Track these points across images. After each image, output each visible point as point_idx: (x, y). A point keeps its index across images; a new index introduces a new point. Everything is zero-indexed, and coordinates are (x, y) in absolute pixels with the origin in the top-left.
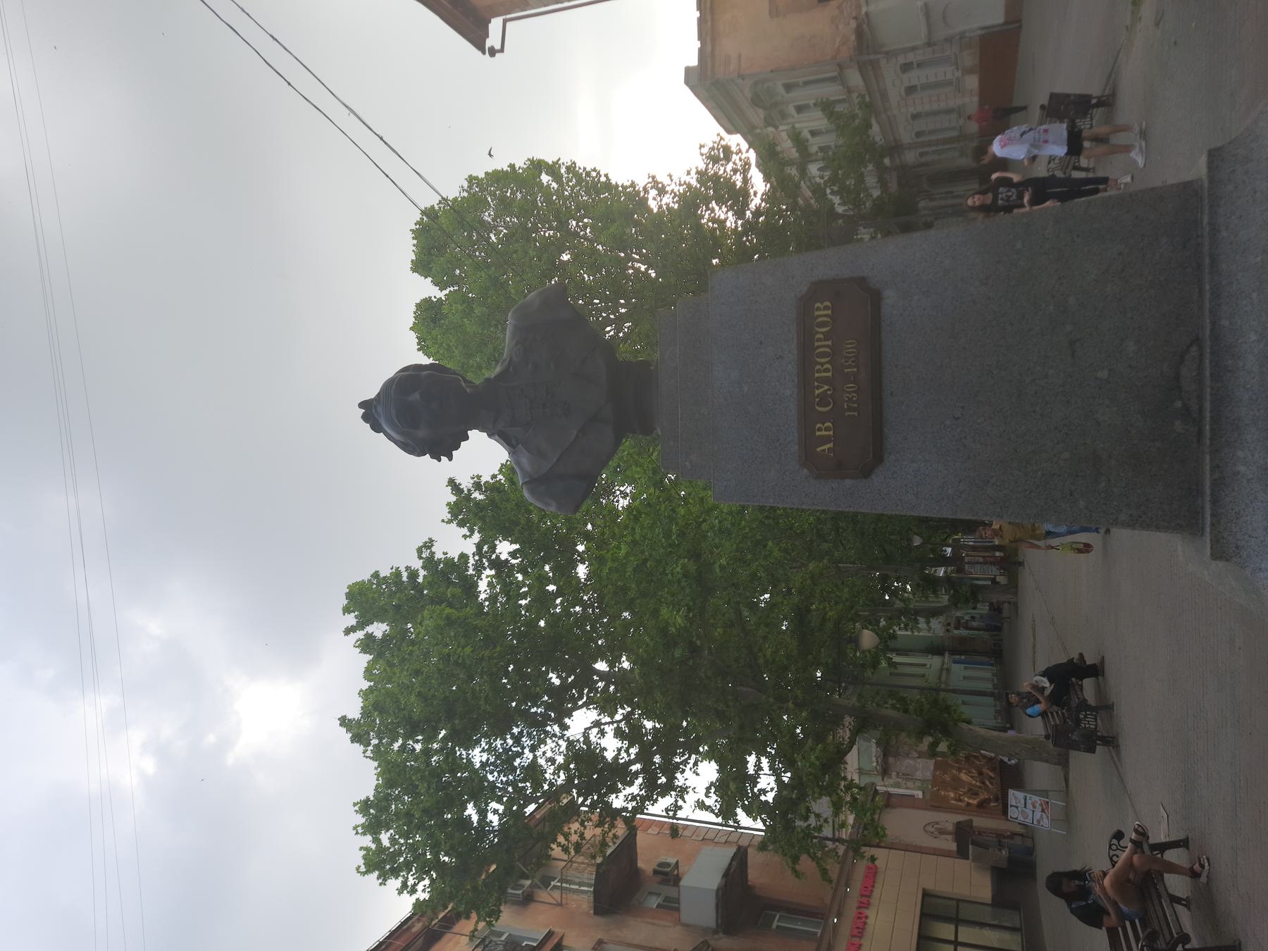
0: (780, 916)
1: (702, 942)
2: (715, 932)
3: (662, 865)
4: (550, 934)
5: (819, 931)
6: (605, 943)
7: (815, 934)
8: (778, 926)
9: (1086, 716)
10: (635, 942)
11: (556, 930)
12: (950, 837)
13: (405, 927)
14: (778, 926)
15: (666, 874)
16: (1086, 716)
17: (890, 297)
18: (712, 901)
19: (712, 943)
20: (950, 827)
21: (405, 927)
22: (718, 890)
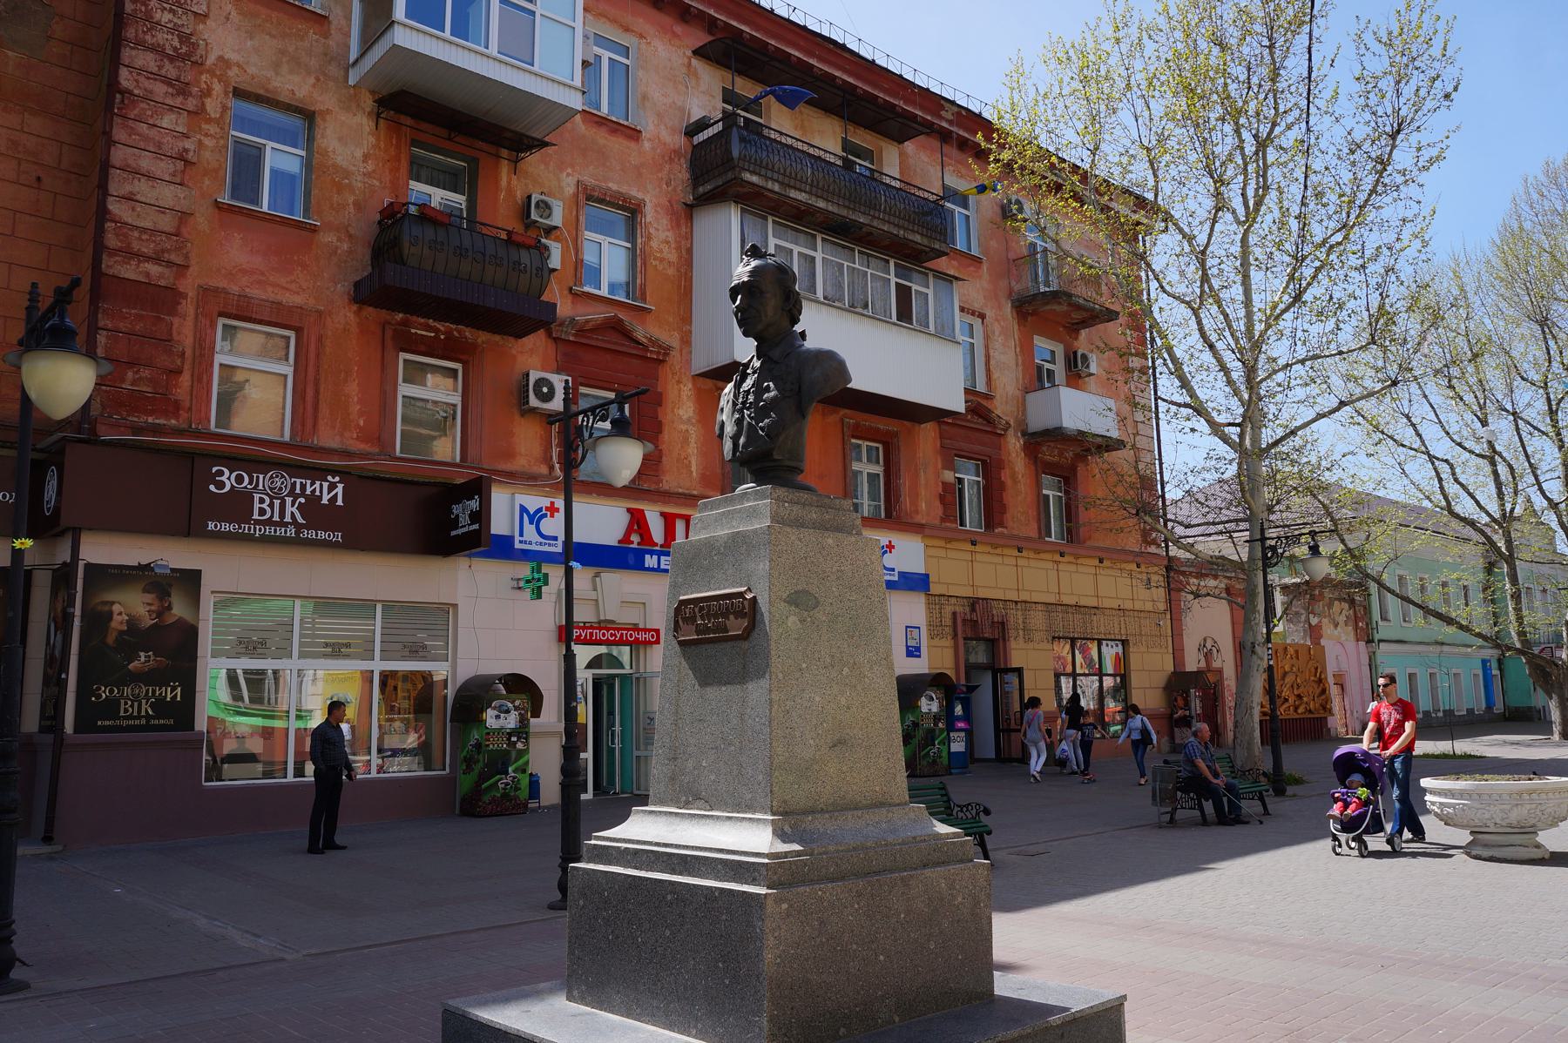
0: (1060, 497)
1: (1007, 423)
2: (1024, 434)
3: (1085, 357)
4: (977, 260)
5: (1053, 539)
6: (983, 323)
7: (1050, 537)
8: (1048, 496)
9: (1192, 799)
10: (991, 352)
11: (985, 267)
12: (1203, 664)
13: (942, 102)
14: (1048, 496)
15: (1076, 366)
16: (1192, 799)
17: (745, 645)
18: (1050, 424)
19: (1011, 432)
20: (1216, 664)
21: (942, 102)
22: (1060, 428)
